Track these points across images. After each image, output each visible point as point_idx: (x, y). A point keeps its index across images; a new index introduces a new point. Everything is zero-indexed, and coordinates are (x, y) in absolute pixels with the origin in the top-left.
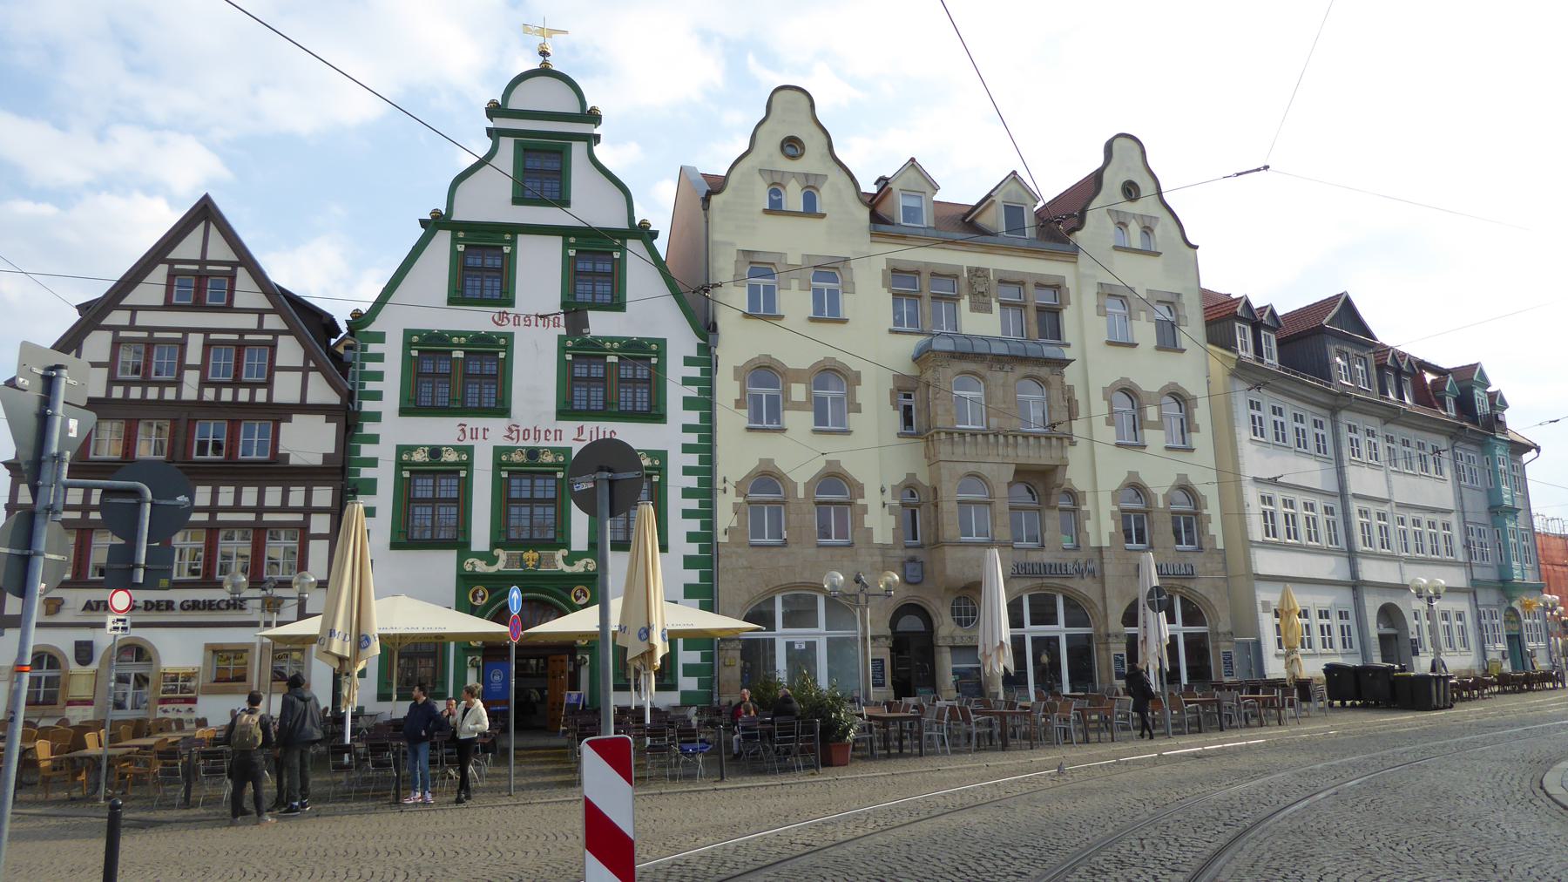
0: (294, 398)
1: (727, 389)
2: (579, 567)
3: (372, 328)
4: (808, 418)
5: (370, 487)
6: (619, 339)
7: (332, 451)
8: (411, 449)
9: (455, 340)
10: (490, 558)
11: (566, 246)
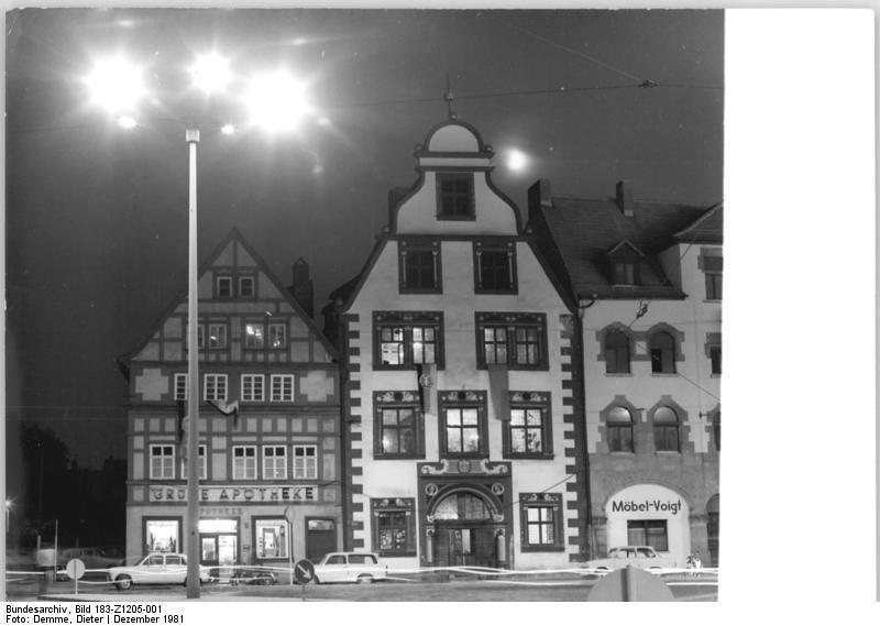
0: (307, 360)
1: (592, 347)
2: (496, 470)
3: (351, 311)
4: (648, 365)
5: (357, 420)
6: (515, 314)
7: (332, 393)
8: (383, 393)
9: (406, 318)
10: (439, 466)
11: (475, 249)
